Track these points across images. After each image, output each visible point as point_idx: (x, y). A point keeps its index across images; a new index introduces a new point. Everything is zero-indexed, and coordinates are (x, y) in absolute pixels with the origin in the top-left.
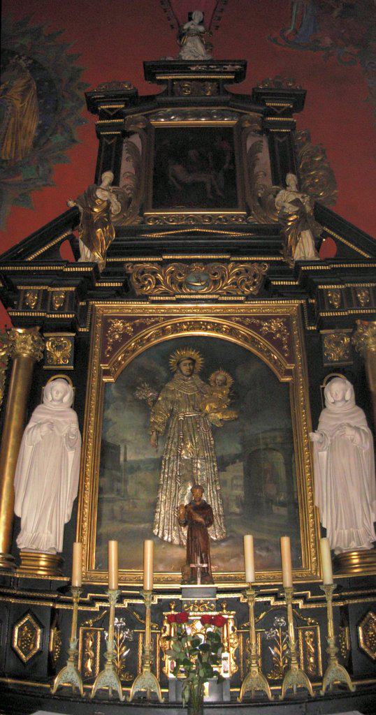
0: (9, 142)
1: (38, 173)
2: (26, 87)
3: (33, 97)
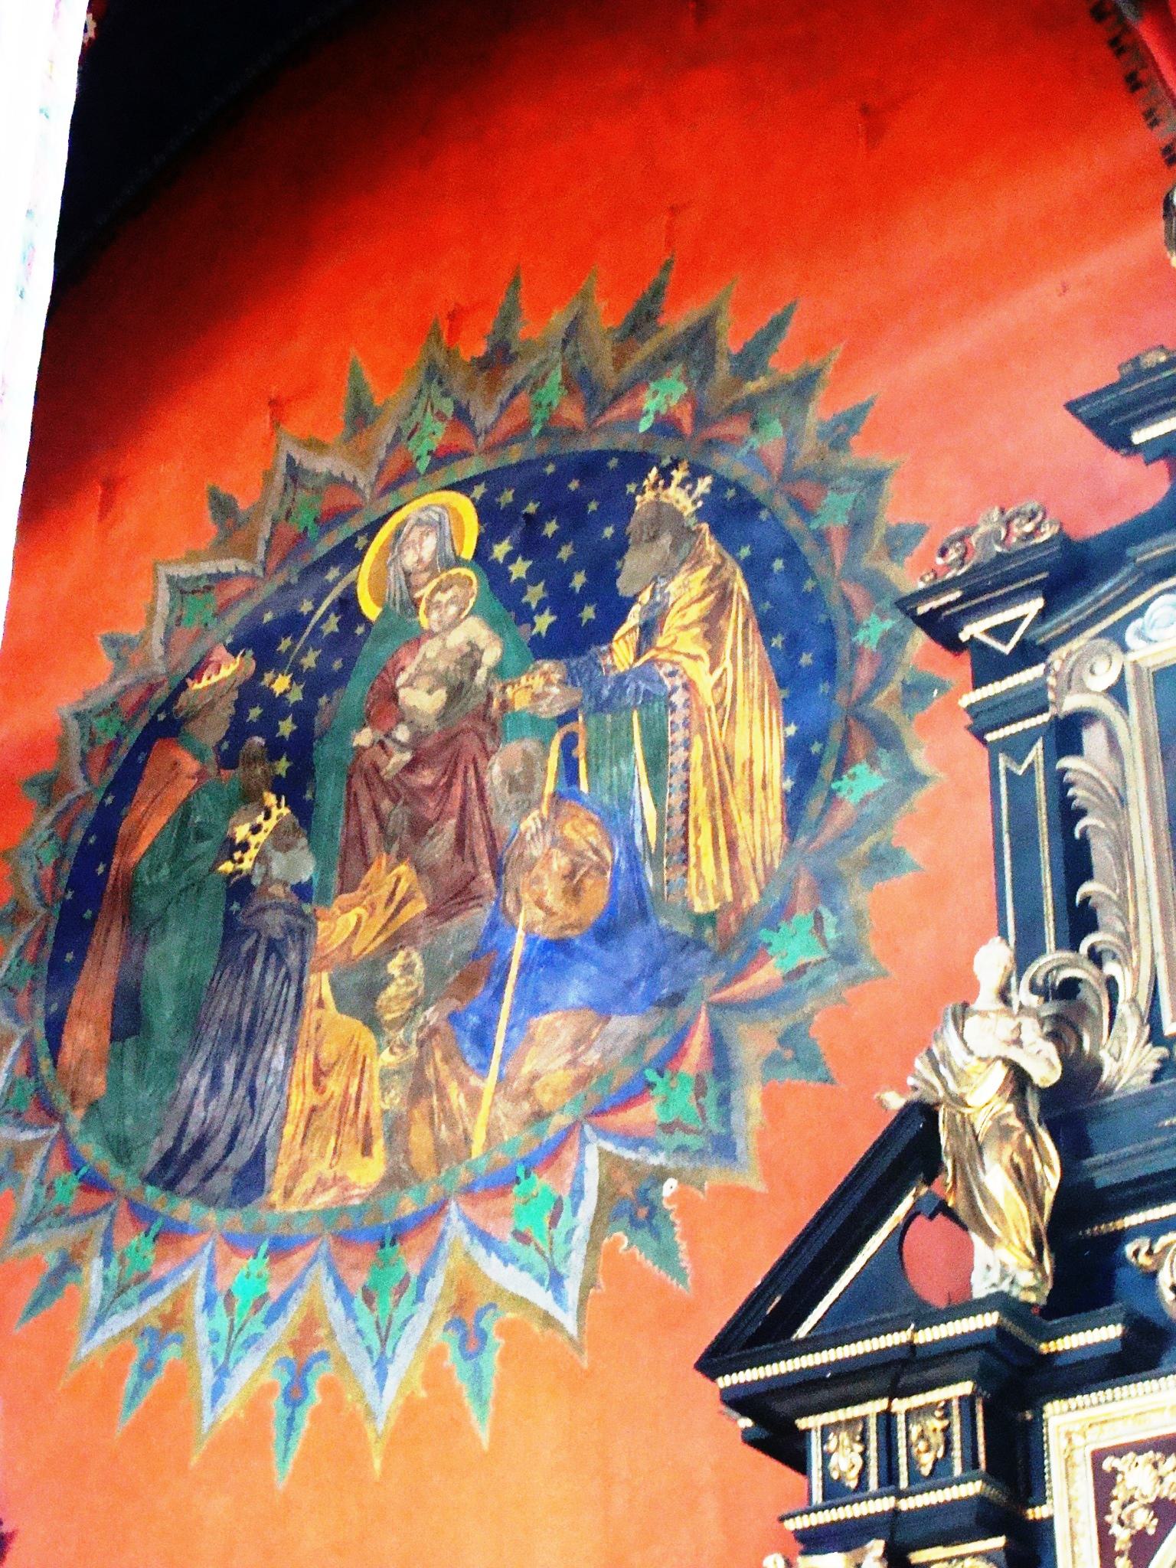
0: (705, 840)
1: (824, 942)
2: (711, 598)
3: (745, 625)
